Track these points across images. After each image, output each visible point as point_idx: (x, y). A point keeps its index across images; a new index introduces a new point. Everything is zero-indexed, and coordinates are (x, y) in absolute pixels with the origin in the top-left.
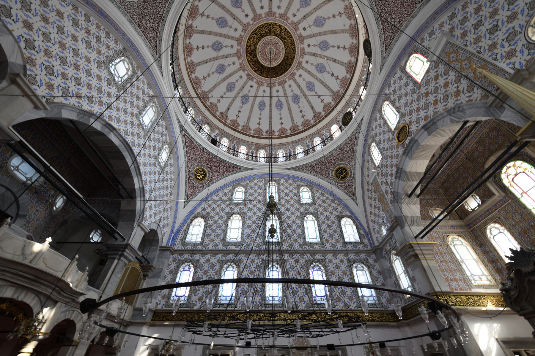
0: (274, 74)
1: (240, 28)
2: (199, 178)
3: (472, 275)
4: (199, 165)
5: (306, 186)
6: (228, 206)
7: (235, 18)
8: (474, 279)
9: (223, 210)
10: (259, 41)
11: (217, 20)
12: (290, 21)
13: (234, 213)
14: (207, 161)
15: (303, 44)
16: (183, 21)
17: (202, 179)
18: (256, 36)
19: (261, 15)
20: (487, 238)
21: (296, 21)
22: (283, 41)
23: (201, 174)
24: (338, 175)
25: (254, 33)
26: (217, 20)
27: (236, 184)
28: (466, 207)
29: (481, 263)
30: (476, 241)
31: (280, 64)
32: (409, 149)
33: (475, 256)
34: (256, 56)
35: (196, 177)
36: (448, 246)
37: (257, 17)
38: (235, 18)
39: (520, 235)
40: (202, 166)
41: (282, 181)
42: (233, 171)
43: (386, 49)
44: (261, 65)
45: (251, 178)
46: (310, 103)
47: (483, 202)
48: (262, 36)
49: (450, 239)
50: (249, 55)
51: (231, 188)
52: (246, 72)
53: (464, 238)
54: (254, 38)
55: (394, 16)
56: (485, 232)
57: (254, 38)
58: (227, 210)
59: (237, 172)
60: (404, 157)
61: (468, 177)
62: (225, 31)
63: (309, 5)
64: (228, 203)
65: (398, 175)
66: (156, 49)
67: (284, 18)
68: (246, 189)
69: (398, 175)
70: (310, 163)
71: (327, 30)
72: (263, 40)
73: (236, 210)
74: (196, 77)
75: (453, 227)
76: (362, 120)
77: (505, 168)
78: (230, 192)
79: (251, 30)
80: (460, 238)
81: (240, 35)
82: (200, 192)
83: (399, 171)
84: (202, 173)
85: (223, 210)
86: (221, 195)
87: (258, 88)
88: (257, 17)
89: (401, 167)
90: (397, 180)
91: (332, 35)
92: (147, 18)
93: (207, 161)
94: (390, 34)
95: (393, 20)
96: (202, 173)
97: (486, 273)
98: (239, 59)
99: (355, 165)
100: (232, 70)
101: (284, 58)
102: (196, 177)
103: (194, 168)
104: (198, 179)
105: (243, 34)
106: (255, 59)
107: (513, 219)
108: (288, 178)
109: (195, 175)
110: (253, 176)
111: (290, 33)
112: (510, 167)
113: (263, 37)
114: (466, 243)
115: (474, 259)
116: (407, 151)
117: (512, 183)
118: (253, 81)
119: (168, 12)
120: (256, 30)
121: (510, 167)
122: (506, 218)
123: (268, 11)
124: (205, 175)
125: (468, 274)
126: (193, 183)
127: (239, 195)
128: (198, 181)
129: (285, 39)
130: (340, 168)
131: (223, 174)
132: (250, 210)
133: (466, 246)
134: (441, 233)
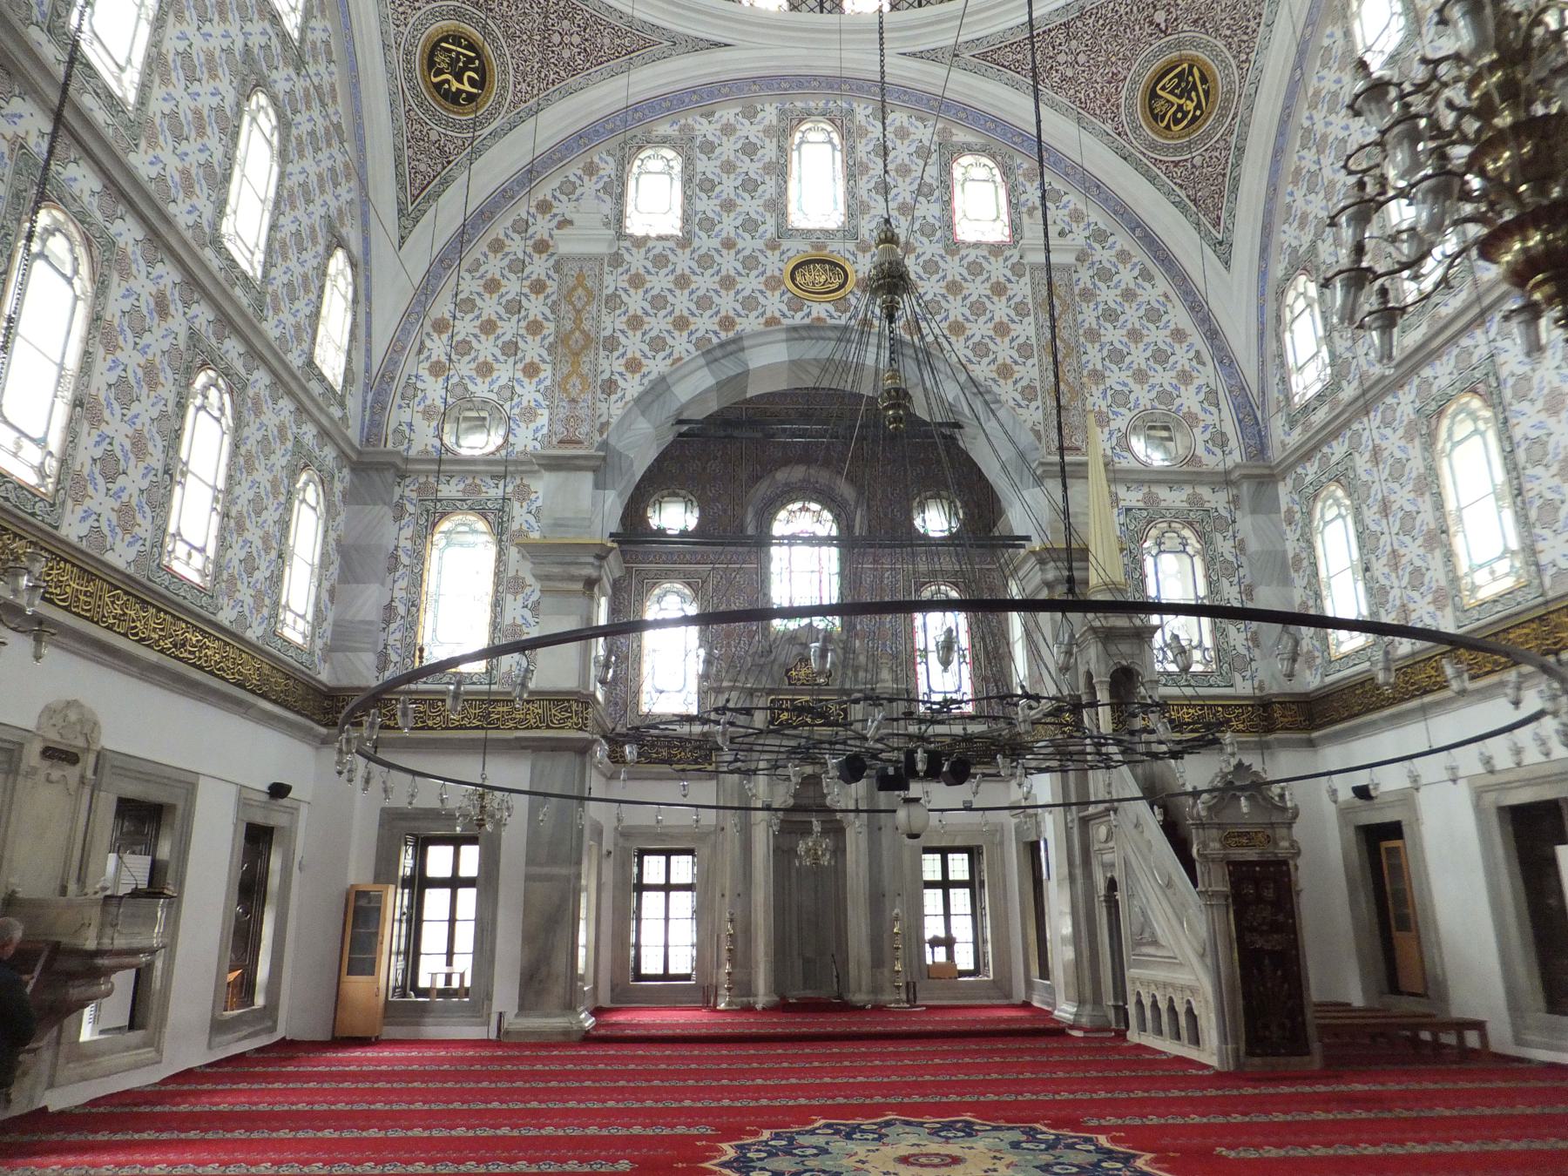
32: (815, 334)
43: (984, 56)
55: (1082, 58)
60: (783, 336)
65: (718, 353)
69: (718, 353)
76: (717, 45)
83: (733, 347)
89: (746, 343)
90: (702, 361)
116: (805, 334)
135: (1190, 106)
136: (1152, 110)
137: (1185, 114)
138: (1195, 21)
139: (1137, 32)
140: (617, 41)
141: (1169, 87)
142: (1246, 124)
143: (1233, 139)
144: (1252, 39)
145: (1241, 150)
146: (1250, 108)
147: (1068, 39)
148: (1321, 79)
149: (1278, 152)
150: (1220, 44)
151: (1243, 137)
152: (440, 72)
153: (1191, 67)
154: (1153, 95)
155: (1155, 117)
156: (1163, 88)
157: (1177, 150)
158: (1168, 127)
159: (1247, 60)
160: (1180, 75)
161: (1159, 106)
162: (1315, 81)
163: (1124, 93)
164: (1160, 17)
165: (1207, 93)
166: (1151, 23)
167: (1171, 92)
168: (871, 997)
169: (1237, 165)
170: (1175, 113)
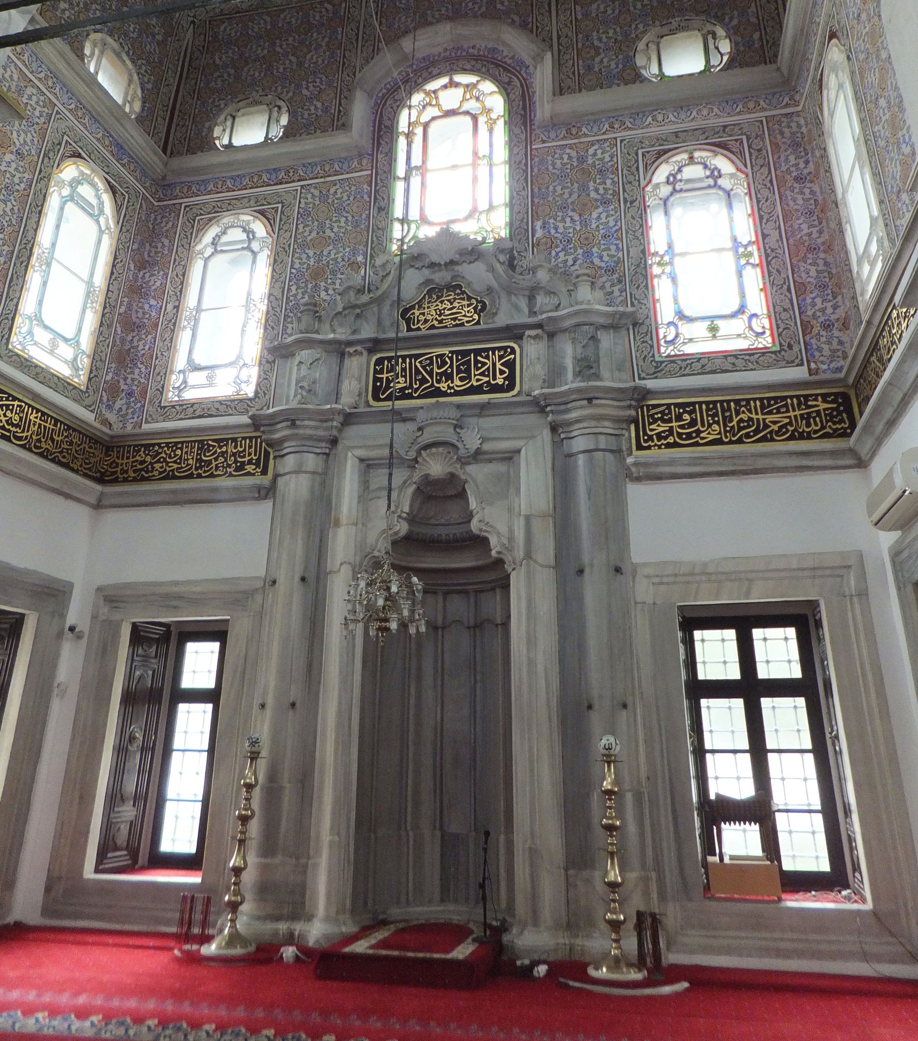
3: (38, 318)
8: (30, 333)
20: (189, 247)
28: (217, 132)
29: (99, 307)
30: (142, 244)
33: (100, 279)
36: (45, 178)
39: (297, 277)
47: (290, 133)
49: (69, 171)
53: (118, 208)
56: (203, 229)
61: (319, 46)
75: (120, 149)
77: (445, 80)
80: (107, 198)
97: (86, 342)
107: (322, 226)
112: (457, 85)
114: (112, 224)
115: (90, 283)
117: (419, 131)
121: (457, 85)
122: (304, 215)
125: (28, 305)
133: (101, 232)
134: (62, 126)
168: (563, 939)
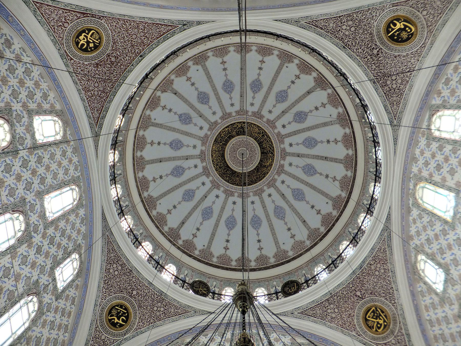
0: (217, 160)
1: (272, 117)
2: (81, 38)
4: (108, 40)
5: (81, 262)
6: (24, 106)
7: (284, 113)
9: (15, 94)
10: (255, 139)
11: (285, 92)
12: (276, 177)
13: (12, 125)
14: (116, 57)
15: (254, 195)
16: (278, 43)
17: (77, 43)
18: (261, 136)
19: (283, 143)
21: (276, 184)
22: (255, 169)
23: (88, 42)
24: (114, 312)
25: (264, 134)
26: (285, 92)
27: (65, 116)
31: (229, 167)
34: (238, 134)
35: (84, 31)
37: (282, 138)
38: (284, 113)
40: (106, 48)
41: (82, 212)
42: (92, 109)
44: (227, 142)
45: (79, 150)
46: (187, 217)
48: (260, 144)
50: (240, 125)
51: (58, 107)
52: (219, 121)
54: (259, 133)
57: (259, 133)
58: (17, 107)
59: (89, 117)
62: (272, 99)
63: (295, 199)
64: (33, 106)
66: (313, 24)
67: (280, 170)
68: (61, 142)
70: (123, 254)
71: (273, 224)
72: (256, 144)
73: (20, 130)
74: (229, 52)
78: (52, 106)
79: (268, 130)
81: (264, 117)
82: (49, 36)
84: (91, 45)
85: (15, 94)
86: (44, 86)
87: (199, 138)
88: (282, 138)
91: (269, 230)
92: (353, 29)
93: (116, 57)
94: (318, 312)
95: (332, 311)
96: (91, 45)
98: (236, 112)
99: (142, 333)
100: (223, 101)
101: (236, 172)
102: (84, 31)
103: (105, 29)
104: (80, 34)
105: (265, 120)
106: (234, 133)
108: (88, 220)
109: (90, 30)
110: (84, 151)
111: (263, 178)
113: (259, 144)
118: (209, 130)
119: (350, 57)
120: (268, 136)
123: (287, 151)
124: (86, 50)
126: (72, 21)
127: (47, 129)
128: (74, 33)
129: (257, 172)
130: (126, 309)
131: (87, 90)
132: (25, 164)
135: (381, 322)
136: (368, 325)
137: (381, 325)
138: (371, 293)
139: (353, 299)
140: (176, 310)
141: (371, 316)
142: (405, 325)
143: (403, 331)
144: (393, 296)
145: (408, 335)
146: (404, 318)
147: (330, 304)
148: (424, 301)
149: (424, 332)
150: (383, 299)
151: (407, 330)
152: (112, 316)
153: (376, 308)
154: (366, 320)
155: (370, 327)
156: (369, 317)
157: (384, 338)
158: (376, 331)
159: (395, 303)
160: (373, 311)
161: (370, 323)
162: (423, 303)
163: (355, 321)
164: (358, 293)
165: (386, 316)
166: (356, 296)
167: (372, 318)
169: (410, 341)
170: (377, 325)
